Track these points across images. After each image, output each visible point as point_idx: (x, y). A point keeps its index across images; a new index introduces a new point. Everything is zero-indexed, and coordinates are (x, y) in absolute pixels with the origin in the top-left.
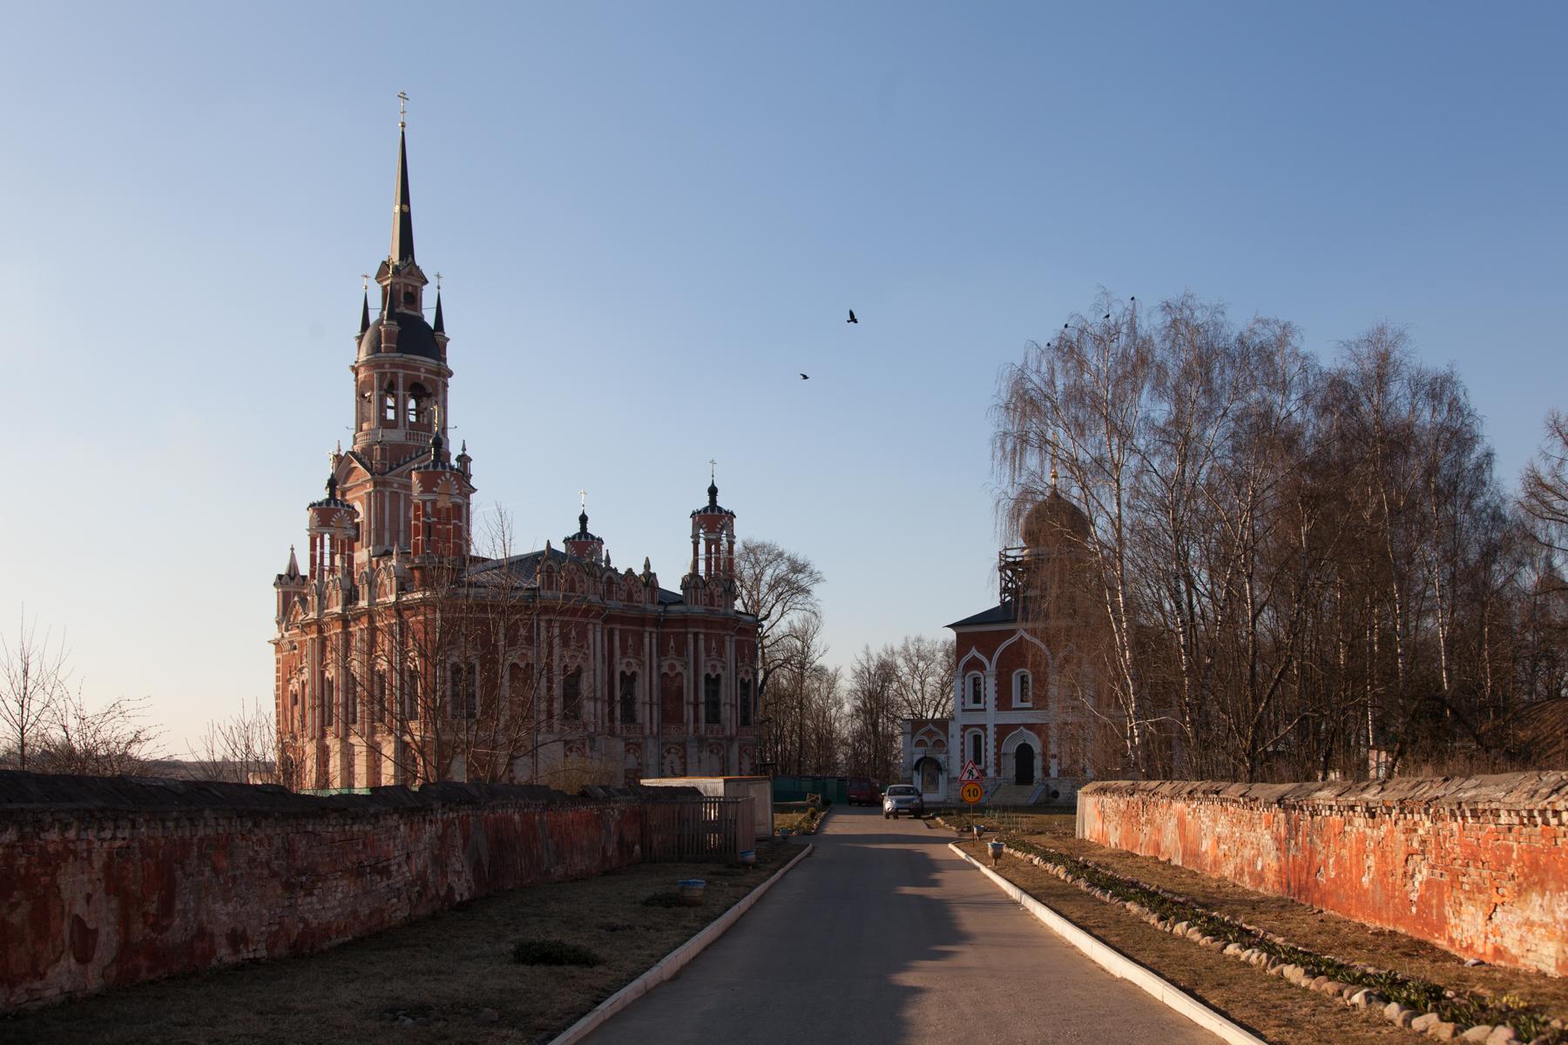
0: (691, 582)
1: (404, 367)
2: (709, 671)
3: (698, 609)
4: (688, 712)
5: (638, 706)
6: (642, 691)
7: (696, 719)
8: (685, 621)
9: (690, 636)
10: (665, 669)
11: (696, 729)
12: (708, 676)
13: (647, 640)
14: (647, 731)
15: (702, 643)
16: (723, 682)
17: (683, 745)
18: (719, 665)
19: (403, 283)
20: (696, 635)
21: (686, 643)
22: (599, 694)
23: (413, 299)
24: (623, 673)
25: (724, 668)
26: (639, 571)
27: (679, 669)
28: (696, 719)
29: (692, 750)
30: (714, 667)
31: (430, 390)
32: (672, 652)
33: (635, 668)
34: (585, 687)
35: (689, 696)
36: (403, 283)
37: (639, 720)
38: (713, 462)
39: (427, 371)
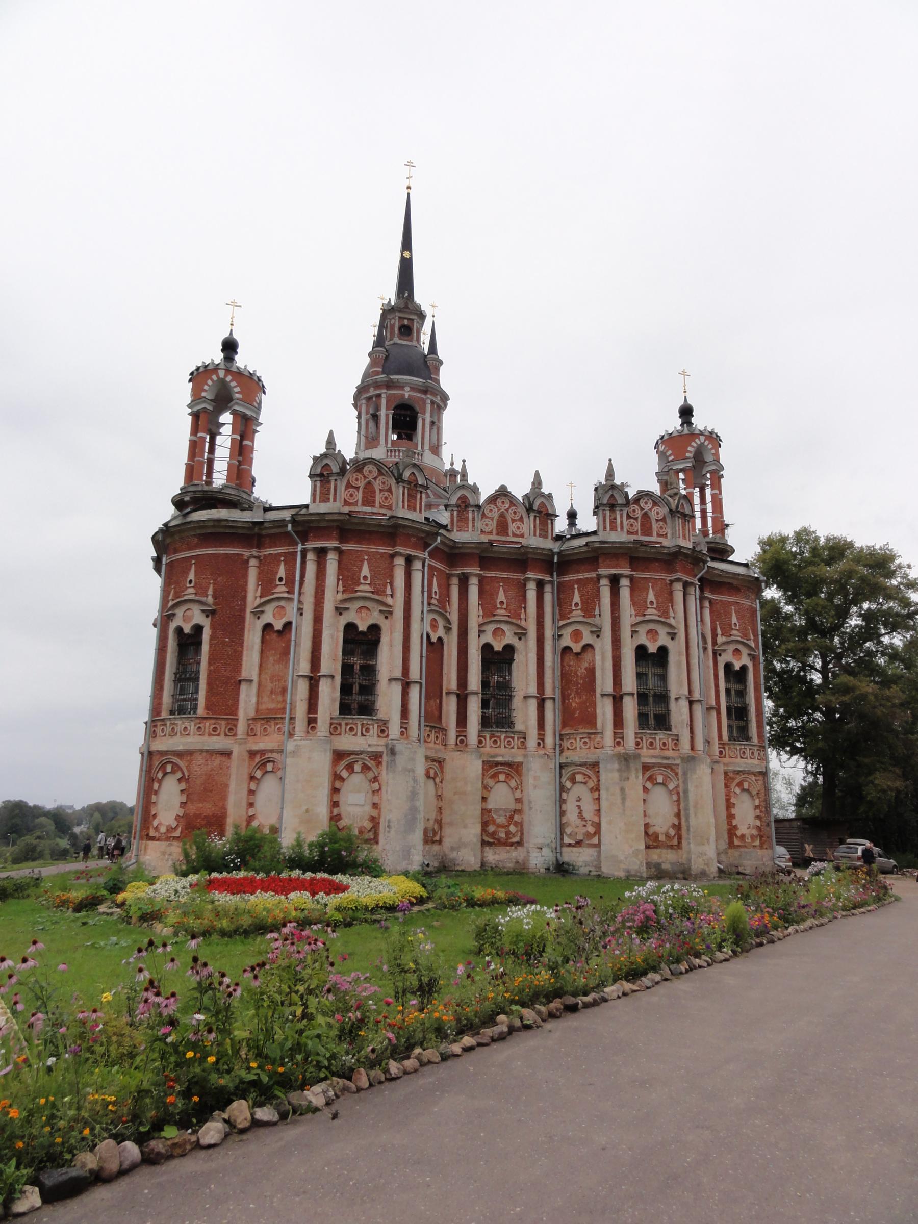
0: (610, 497)
1: (389, 385)
2: (643, 639)
3: (618, 537)
4: (605, 710)
5: (517, 703)
6: (523, 676)
7: (618, 721)
8: (595, 555)
9: (604, 582)
10: (566, 641)
11: (619, 738)
12: (641, 651)
13: (531, 595)
14: (532, 742)
15: (625, 593)
16: (672, 658)
17: (595, 766)
18: (662, 631)
19: (402, 318)
20: (615, 581)
21: (597, 595)
22: (415, 673)
23: (407, 331)
24: (487, 649)
25: (673, 636)
26: (520, 489)
27: (587, 638)
28: (618, 721)
29: (609, 775)
30: (652, 633)
31: (418, 409)
32: (577, 614)
33: (509, 638)
34: (388, 660)
35: (604, 682)
36: (402, 318)
37: (519, 726)
38: (684, 373)
39: (412, 389)
